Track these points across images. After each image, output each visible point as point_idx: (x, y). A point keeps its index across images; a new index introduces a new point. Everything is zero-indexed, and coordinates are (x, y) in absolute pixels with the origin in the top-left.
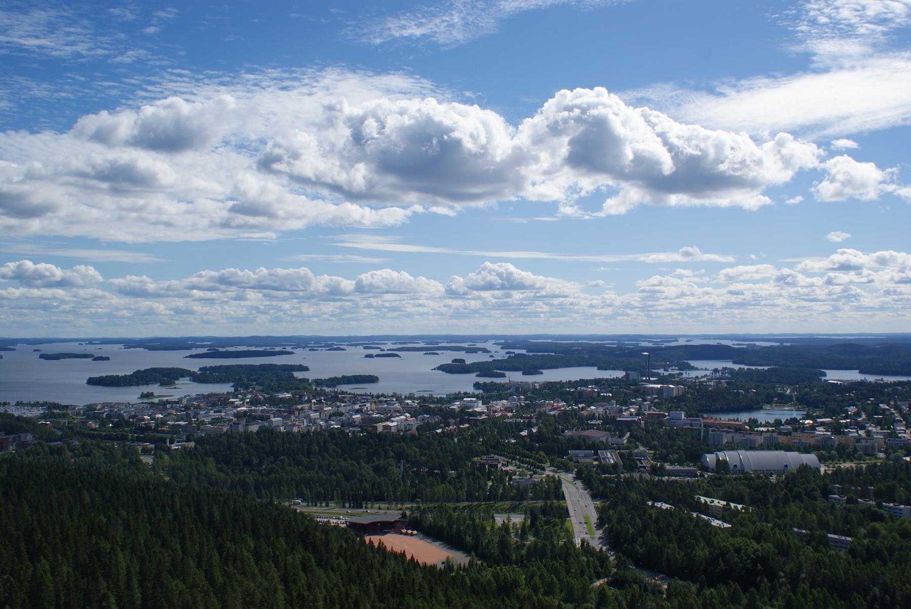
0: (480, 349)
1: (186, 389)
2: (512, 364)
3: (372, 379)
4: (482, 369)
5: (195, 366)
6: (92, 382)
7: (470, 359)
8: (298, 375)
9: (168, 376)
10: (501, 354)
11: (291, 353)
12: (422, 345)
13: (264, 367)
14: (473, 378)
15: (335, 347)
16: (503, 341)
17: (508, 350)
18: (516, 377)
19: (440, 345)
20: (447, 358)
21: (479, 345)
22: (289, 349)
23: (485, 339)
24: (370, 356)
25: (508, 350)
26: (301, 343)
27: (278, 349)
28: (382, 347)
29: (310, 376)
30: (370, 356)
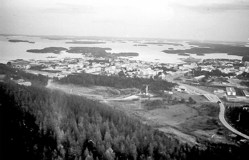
0: (180, 45)
1: (64, 55)
2: (193, 51)
3: (136, 55)
4: (180, 52)
5: (68, 46)
6: (28, 51)
7: (175, 48)
8: (107, 51)
9: (56, 50)
10: (188, 47)
11: (105, 43)
12: (156, 42)
13: (94, 48)
14: (176, 56)
15: (122, 41)
16: (189, 42)
17: (191, 46)
18: (194, 56)
19: (164, 42)
20: (167, 47)
21: (179, 43)
22: (104, 41)
23: (182, 41)
24: (136, 45)
25: (191, 46)
26: (109, 39)
27: (100, 41)
28: (141, 42)
29: (112, 52)
30: (136, 45)
